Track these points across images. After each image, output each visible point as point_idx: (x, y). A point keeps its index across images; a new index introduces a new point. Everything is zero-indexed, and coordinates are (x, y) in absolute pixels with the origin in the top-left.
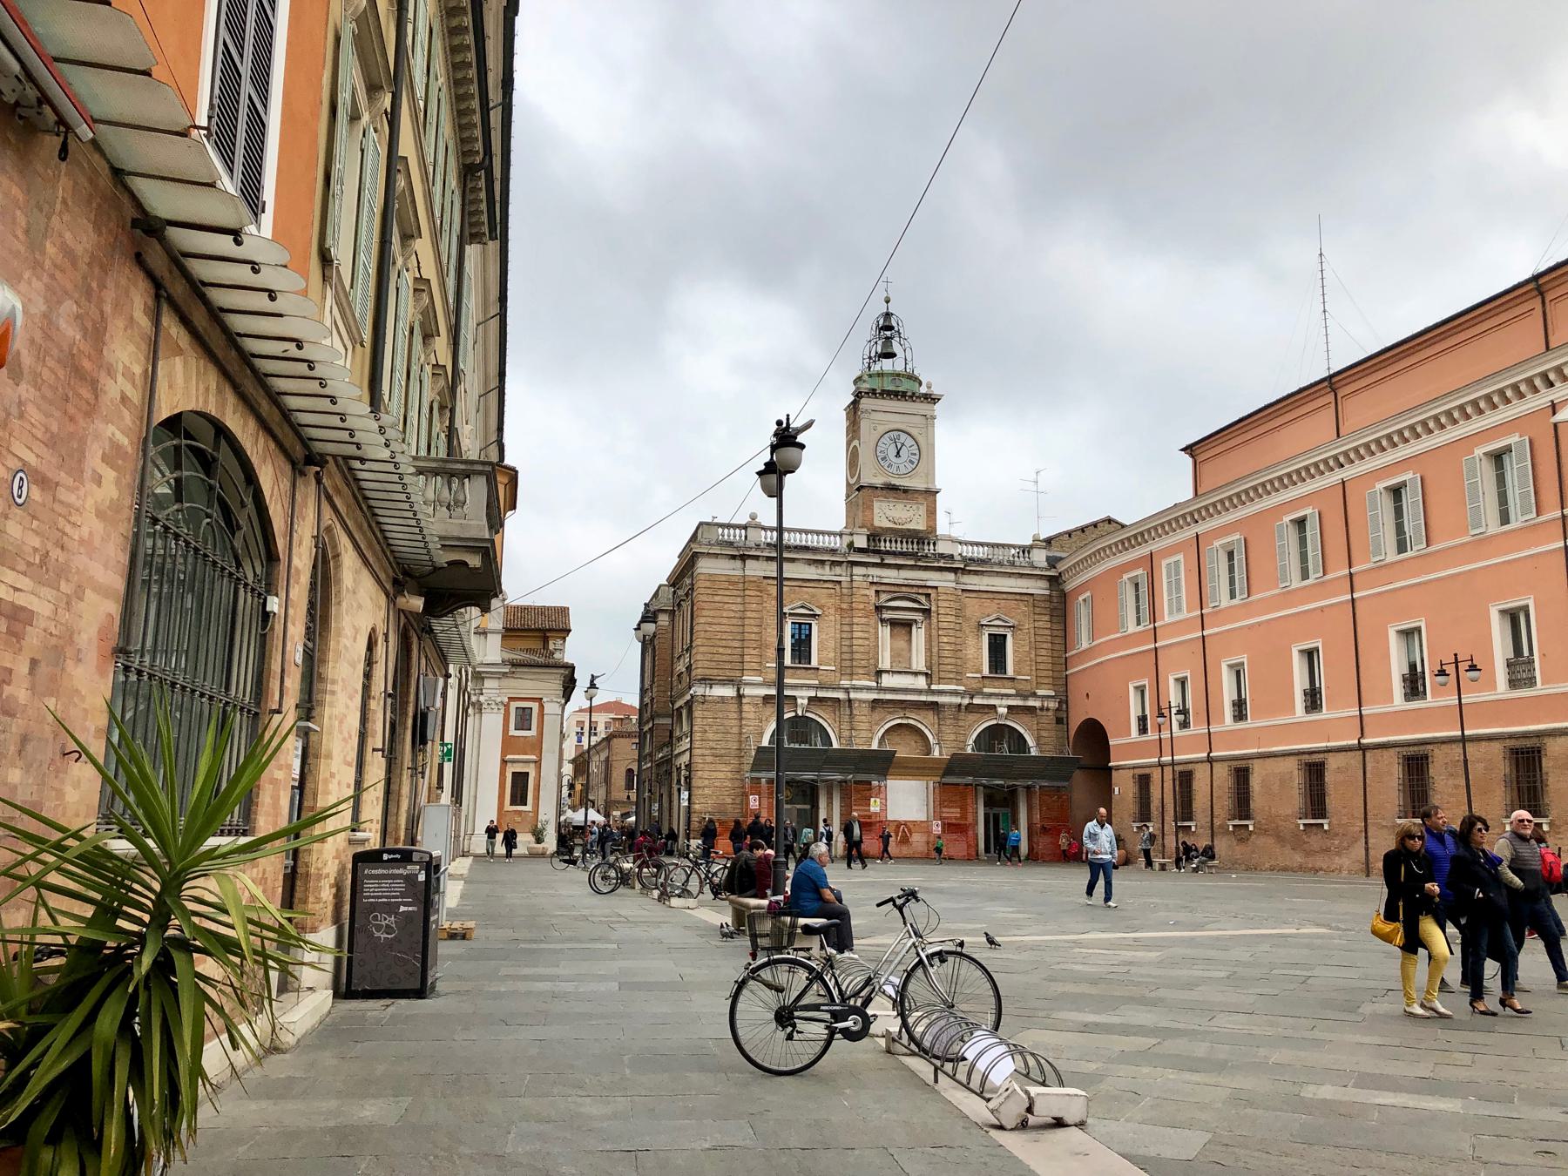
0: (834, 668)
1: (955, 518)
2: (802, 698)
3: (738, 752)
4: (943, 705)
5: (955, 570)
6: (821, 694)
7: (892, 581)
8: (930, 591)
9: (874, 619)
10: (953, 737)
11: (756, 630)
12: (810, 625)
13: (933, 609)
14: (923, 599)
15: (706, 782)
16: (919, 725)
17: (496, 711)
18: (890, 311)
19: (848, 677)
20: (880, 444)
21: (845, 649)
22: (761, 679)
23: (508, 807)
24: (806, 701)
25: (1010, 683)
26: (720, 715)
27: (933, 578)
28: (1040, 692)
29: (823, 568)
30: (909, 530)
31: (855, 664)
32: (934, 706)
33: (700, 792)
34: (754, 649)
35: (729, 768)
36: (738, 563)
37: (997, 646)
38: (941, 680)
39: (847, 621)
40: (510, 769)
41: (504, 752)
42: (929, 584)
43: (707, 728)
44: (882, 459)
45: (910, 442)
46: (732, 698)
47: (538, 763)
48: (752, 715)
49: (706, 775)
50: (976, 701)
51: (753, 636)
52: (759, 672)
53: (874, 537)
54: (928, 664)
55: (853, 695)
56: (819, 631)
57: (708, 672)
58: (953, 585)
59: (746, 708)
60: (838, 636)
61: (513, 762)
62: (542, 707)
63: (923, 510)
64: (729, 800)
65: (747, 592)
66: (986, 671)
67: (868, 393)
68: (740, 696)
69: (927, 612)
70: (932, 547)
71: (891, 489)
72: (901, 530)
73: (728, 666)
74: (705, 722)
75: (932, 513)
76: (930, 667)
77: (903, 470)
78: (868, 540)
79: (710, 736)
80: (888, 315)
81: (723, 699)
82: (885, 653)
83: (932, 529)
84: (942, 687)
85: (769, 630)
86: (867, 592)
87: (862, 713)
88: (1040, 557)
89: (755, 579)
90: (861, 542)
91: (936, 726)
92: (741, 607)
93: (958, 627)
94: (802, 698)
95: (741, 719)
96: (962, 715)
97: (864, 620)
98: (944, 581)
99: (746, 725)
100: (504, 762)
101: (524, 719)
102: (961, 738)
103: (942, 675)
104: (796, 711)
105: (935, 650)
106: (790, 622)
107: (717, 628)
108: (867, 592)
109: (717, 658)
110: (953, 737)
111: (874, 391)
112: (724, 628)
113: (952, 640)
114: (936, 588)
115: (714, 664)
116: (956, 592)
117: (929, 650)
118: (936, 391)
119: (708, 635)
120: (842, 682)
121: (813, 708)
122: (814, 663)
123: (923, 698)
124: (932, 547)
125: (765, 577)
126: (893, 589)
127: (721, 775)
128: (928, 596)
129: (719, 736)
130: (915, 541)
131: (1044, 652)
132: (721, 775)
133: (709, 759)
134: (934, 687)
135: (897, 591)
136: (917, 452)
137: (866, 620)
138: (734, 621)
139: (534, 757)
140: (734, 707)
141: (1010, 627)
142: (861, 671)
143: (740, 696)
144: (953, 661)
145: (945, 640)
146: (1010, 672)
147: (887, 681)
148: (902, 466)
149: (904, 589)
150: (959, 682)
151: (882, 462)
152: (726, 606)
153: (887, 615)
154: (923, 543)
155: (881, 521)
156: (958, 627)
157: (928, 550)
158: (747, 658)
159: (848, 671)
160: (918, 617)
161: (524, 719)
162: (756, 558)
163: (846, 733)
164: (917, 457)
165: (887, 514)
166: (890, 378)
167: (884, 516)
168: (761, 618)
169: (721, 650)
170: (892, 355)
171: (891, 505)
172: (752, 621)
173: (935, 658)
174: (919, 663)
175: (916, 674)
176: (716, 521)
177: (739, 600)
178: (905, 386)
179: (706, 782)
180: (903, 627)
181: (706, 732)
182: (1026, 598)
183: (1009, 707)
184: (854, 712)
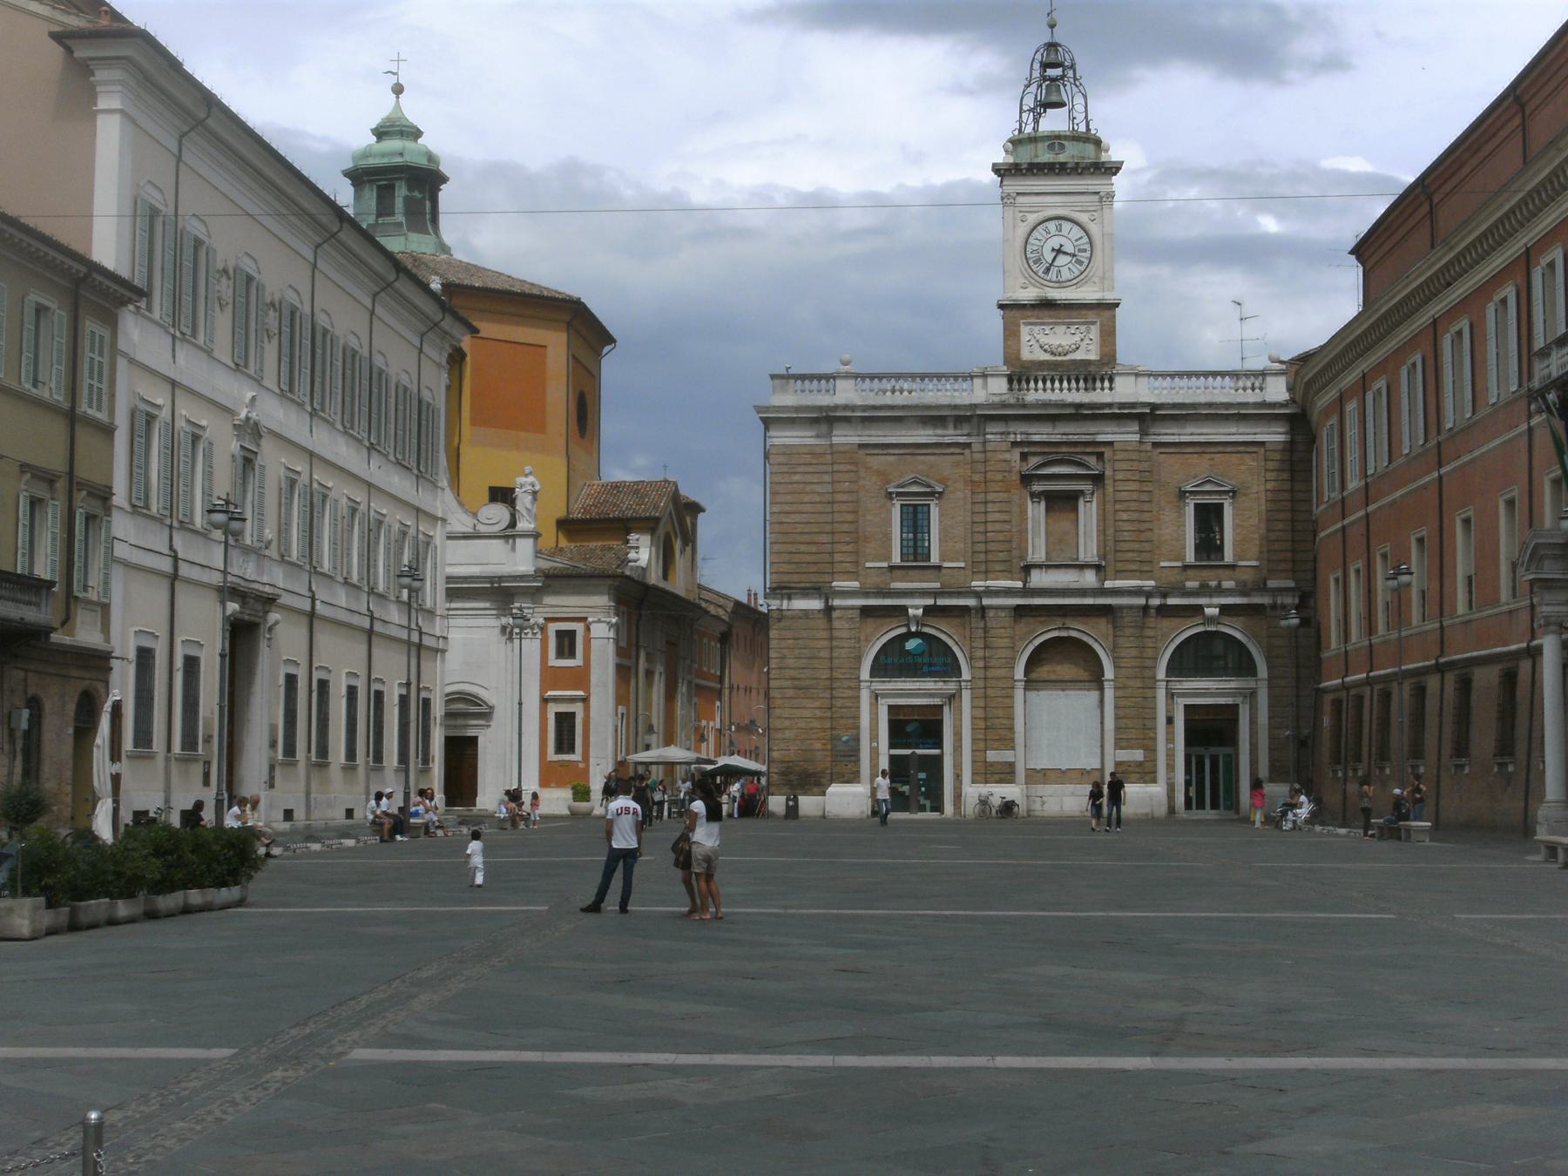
0: (962, 565)
1: (1248, 309)
2: (917, 607)
3: (828, 683)
4: (1121, 608)
5: (1140, 418)
6: (941, 602)
7: (1044, 438)
8: (1102, 449)
9: (1018, 494)
10: (1134, 652)
11: (850, 517)
12: (929, 505)
13: (1107, 473)
14: (1092, 461)
15: (787, 723)
16: (1085, 638)
17: (530, 635)
18: (1057, 39)
19: (983, 576)
20: (1031, 240)
21: (981, 538)
22: (856, 584)
23: (552, 756)
24: (920, 611)
25: (1228, 572)
26: (804, 634)
27: (1108, 433)
28: (1271, 584)
30: (1074, 362)
31: (990, 557)
32: (1106, 611)
33: (780, 735)
34: (848, 543)
35: (817, 704)
36: (824, 428)
37: (1209, 517)
38: (1119, 574)
39: (981, 497)
40: (553, 709)
41: (543, 690)
43: (786, 651)
44: (1035, 263)
45: (1077, 232)
46: (819, 611)
49: (786, 713)
50: (1171, 601)
51: (846, 527)
52: (853, 575)
53: (1020, 375)
54: (1102, 551)
55: (986, 602)
56: (941, 515)
57: (785, 578)
58: (1137, 437)
59: (836, 624)
60: (969, 519)
61: (556, 700)
62: (588, 629)
63: (1095, 332)
64: (818, 745)
65: (836, 467)
66: (1190, 557)
67: (1010, 170)
68: (829, 610)
69: (1098, 479)
70: (1107, 384)
71: (1046, 305)
72: (1061, 363)
73: (814, 568)
74: (784, 644)
75: (1108, 334)
76: (1103, 556)
77: (1066, 275)
78: (1010, 381)
79: (790, 662)
80: (1052, 46)
81: (806, 614)
82: (1037, 540)
83: (1109, 357)
84: (1119, 583)
85: (869, 517)
86: (1007, 456)
87: (1001, 627)
88: (1277, 390)
89: (846, 448)
90: (999, 386)
91: (1111, 638)
92: (829, 488)
93: (1145, 497)
94: (917, 607)
95: (831, 639)
96: (1151, 621)
97: (1003, 496)
98: (1127, 435)
99: (837, 647)
100: (545, 701)
101: (566, 644)
102: (1149, 653)
103: (1120, 566)
104: (908, 626)
105: (1110, 531)
106: (897, 504)
107: (797, 518)
108: (1007, 456)
109: (797, 558)
110: (1134, 652)
112: (804, 518)
113: (1135, 516)
114: (1111, 443)
115: (793, 566)
116: (1144, 447)
117: (1102, 532)
118: (1114, 155)
120: (974, 583)
121: (931, 621)
122: (935, 559)
123: (1089, 601)
124: (1107, 384)
125: (861, 446)
126: (1047, 450)
127: (807, 713)
128: (1100, 456)
129: (803, 662)
130: (1081, 377)
131: (1280, 526)
132: (807, 713)
133: (790, 693)
134: (1108, 584)
135: (1054, 453)
136: (1087, 247)
137: (1006, 495)
138: (819, 508)
139: (581, 693)
140: (822, 623)
141: (1226, 492)
142: (998, 567)
144: (1136, 546)
145: (1125, 516)
146: (1229, 557)
147: (1038, 579)
148: (1065, 271)
149: (1064, 449)
150: (1142, 574)
151: (1034, 267)
152: (808, 488)
153: (1037, 487)
154: (1094, 381)
156: (1145, 497)
157: (1101, 396)
158: (838, 557)
159: (983, 568)
160: (1086, 487)
161: (566, 644)
162: (847, 420)
163: (980, 653)
164: (1088, 254)
165: (1039, 341)
166: (1047, 144)
167: (1036, 346)
168: (857, 501)
169: (803, 548)
170: (1061, 105)
171: (1047, 329)
172: (844, 507)
173: (1111, 543)
174: (1089, 550)
175: (1082, 567)
176: (791, 372)
177: (827, 478)
178: (1070, 154)
179: (787, 723)
180: (1062, 503)
181: (784, 657)
182: (1255, 449)
183: (1224, 609)
184: (989, 625)
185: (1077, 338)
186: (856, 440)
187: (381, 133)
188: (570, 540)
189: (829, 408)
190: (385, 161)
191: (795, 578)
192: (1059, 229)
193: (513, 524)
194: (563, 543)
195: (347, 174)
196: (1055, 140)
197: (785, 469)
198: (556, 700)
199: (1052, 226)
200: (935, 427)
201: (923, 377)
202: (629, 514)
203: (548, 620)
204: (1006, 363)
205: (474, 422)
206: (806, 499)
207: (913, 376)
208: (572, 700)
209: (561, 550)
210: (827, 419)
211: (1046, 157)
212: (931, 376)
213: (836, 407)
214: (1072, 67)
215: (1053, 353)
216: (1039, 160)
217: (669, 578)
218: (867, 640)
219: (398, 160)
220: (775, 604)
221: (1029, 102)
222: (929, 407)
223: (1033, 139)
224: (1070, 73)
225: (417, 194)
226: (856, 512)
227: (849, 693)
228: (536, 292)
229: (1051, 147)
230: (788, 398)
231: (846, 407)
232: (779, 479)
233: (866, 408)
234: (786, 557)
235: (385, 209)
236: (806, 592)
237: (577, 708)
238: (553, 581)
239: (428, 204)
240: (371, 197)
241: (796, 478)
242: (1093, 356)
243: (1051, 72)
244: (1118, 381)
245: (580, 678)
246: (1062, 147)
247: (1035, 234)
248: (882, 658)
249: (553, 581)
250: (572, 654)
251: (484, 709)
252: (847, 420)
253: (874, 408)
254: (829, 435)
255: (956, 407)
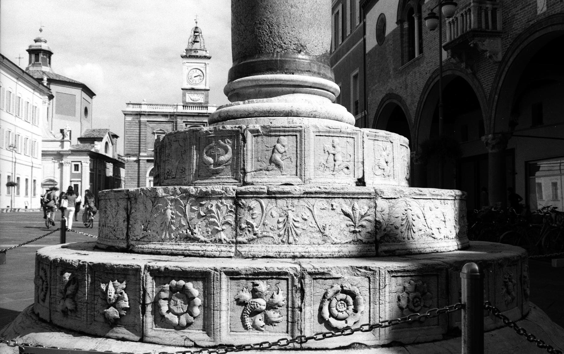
11: (144, 138)
18: (198, 26)
29: (167, 117)
36: (139, 116)
41: (71, 178)
42: (204, 121)
45: (200, 72)
47: (81, 181)
48: (142, 166)
51: (143, 140)
52: (145, 152)
57: (129, 152)
59: (141, 163)
61: (74, 181)
62: (81, 164)
71: (193, 89)
75: (207, 96)
77: (198, 82)
79: (130, 172)
80: (196, 28)
83: (207, 102)
86: (182, 125)
100: (71, 181)
107: (132, 138)
109: (132, 148)
111: (186, 56)
112: (134, 138)
119: (129, 140)
125: (148, 121)
133: (130, 180)
143: (139, 160)
148: (197, 81)
152: (135, 131)
155: (188, 100)
162: (144, 115)
165: (191, 97)
169: (133, 145)
185: (199, 97)
186: (146, 120)
187: (36, 41)
188: (81, 143)
189: (140, 112)
190: (37, 48)
191: (132, 152)
192: (196, 71)
193: (63, 138)
194: (79, 143)
195: (27, 51)
196: (196, 50)
197: (128, 126)
198: (74, 181)
199: (194, 70)
200: (165, 117)
201: (163, 105)
202: (96, 137)
203: (72, 162)
204: (183, 102)
205: (57, 113)
206: (134, 133)
207: (160, 105)
208: (78, 181)
209: (79, 145)
210: (140, 114)
211: (193, 54)
212: (165, 105)
213: (141, 112)
214: (201, 33)
215: (193, 101)
216: (192, 54)
217: (108, 152)
218: (148, 167)
219: (40, 48)
220: (126, 158)
221: (190, 41)
222: (164, 112)
223: (191, 50)
224: (200, 34)
225: (45, 56)
226: (146, 137)
227: (143, 180)
228: (73, 82)
229: (195, 52)
230: (131, 109)
231: (144, 112)
232: (127, 128)
233: (148, 112)
234: (129, 147)
235: (37, 60)
236: (134, 156)
237: (79, 183)
238: (74, 152)
239: (48, 59)
240: (33, 57)
241: (132, 128)
242: (203, 102)
243: (196, 34)
244: (209, 107)
245: (80, 176)
246: (197, 52)
247: (190, 72)
248: (152, 172)
249: (74, 152)
250: (78, 170)
251: (55, 183)
252: (144, 115)
253: (151, 112)
254: (140, 118)
255: (170, 113)
